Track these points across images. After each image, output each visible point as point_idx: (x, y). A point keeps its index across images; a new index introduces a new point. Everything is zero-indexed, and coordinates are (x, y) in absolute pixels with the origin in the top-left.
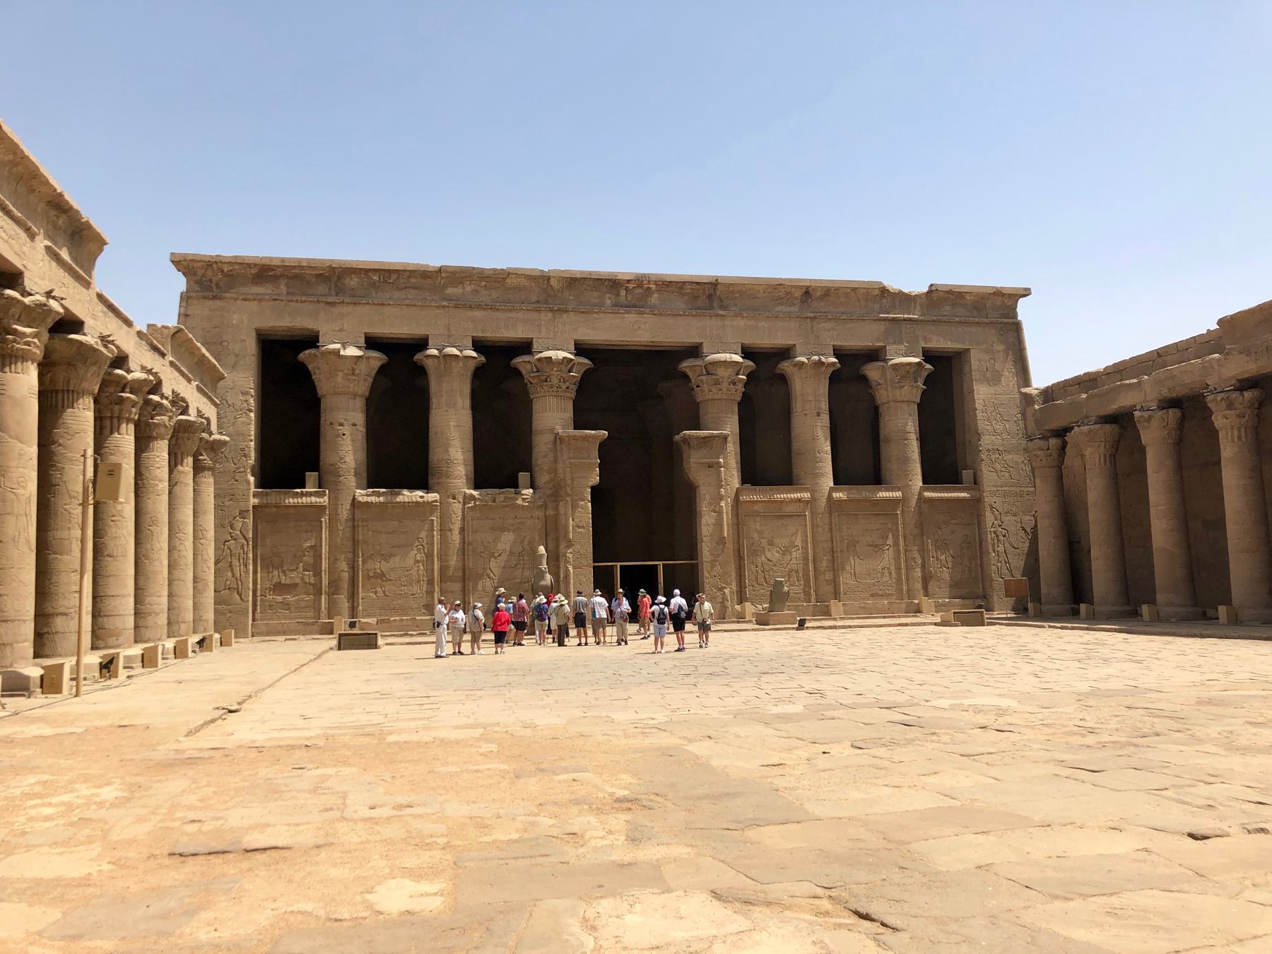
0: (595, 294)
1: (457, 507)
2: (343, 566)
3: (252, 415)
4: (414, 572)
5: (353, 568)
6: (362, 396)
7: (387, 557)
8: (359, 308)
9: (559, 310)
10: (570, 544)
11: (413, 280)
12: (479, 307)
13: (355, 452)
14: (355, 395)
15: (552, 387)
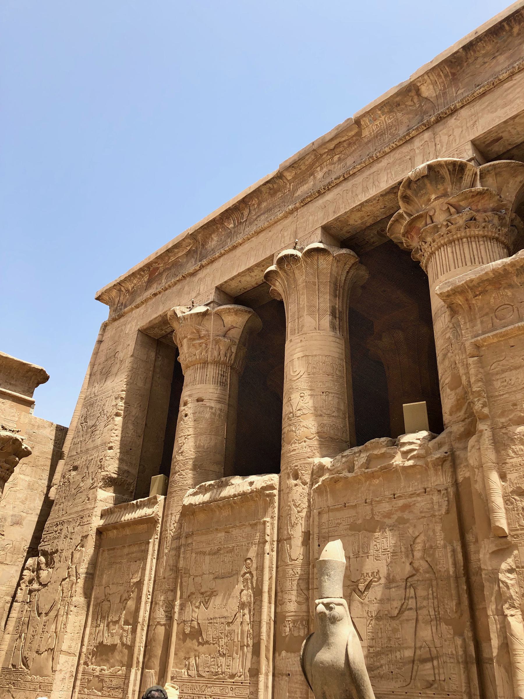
0: (501, 59)
1: (300, 493)
2: (160, 614)
3: (119, 420)
4: (236, 627)
5: (170, 618)
6: (216, 363)
7: (207, 596)
8: (216, 265)
9: (439, 120)
10: (504, 545)
11: (264, 205)
12: (329, 188)
13: (197, 435)
14: (205, 363)
15: (436, 229)
